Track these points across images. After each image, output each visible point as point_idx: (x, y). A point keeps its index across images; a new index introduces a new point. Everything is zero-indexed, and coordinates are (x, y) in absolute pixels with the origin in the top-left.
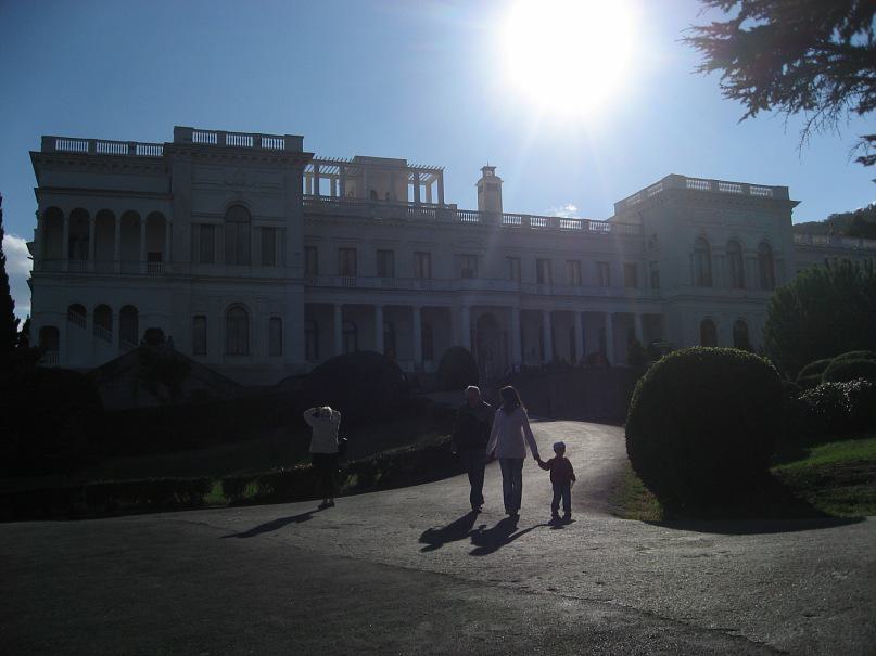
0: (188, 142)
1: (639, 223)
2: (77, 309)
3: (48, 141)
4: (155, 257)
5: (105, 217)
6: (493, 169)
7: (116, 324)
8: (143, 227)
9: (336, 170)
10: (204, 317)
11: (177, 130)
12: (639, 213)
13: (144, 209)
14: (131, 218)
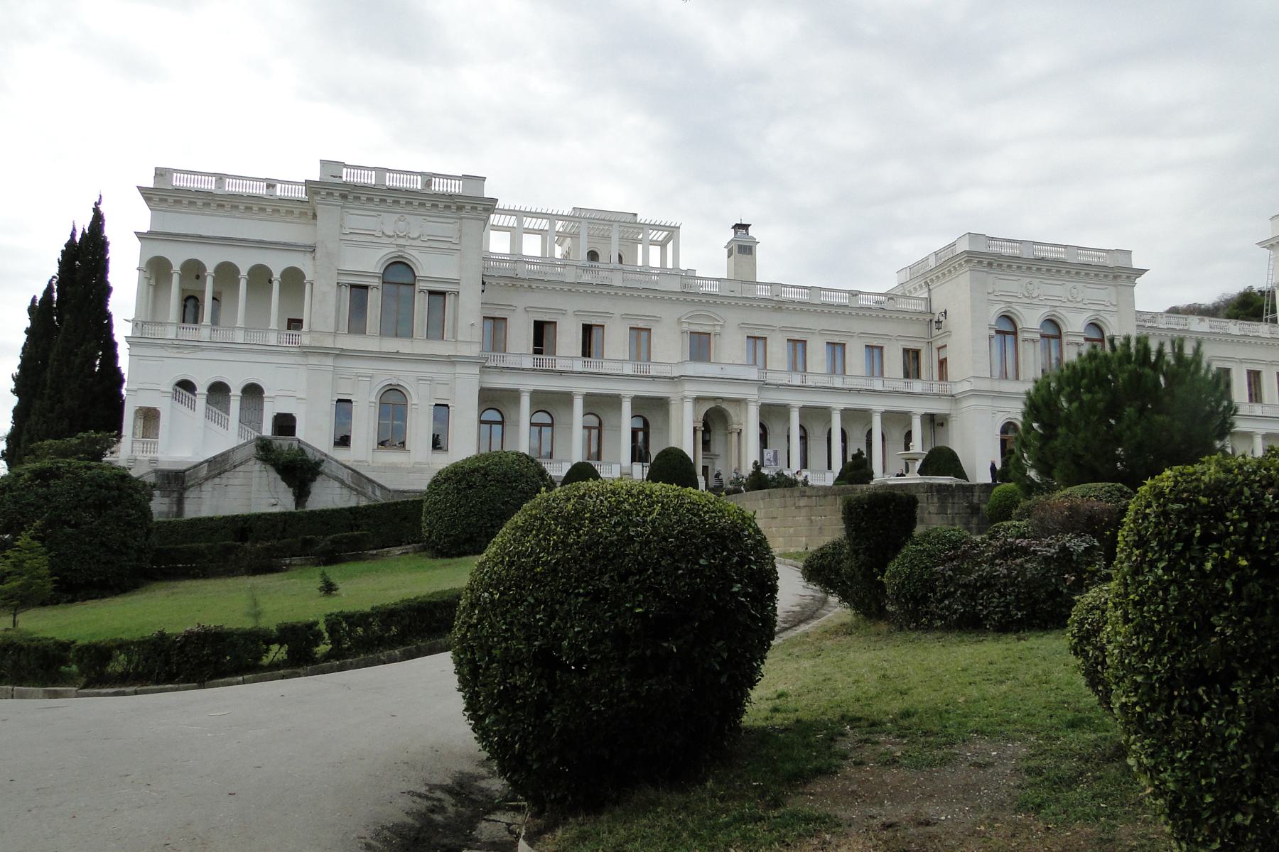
0: (337, 181)
1: (926, 295)
2: (187, 385)
3: (161, 173)
4: (295, 324)
5: (227, 272)
6: (746, 227)
7: (235, 404)
8: (276, 286)
9: (544, 224)
10: (350, 401)
11: (324, 163)
12: (926, 283)
13: (277, 264)
14: (260, 276)
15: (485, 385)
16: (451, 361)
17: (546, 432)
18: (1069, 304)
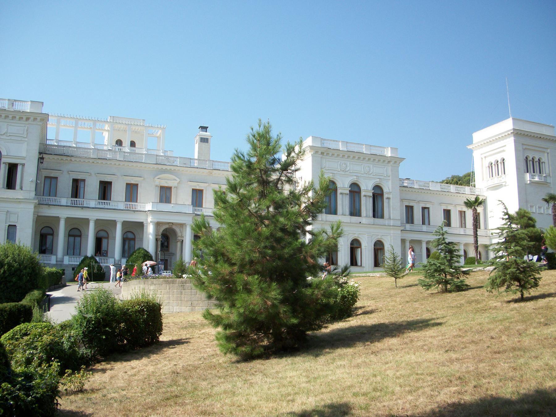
15: (40, 214)
16: (18, 201)
17: (78, 239)
18: (365, 175)
